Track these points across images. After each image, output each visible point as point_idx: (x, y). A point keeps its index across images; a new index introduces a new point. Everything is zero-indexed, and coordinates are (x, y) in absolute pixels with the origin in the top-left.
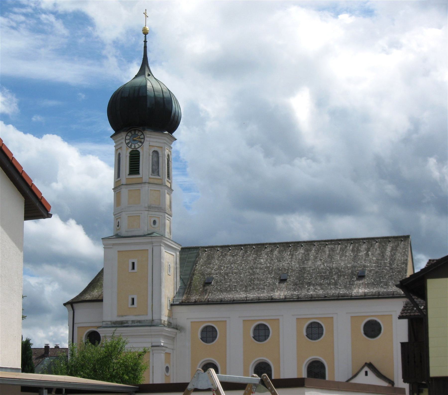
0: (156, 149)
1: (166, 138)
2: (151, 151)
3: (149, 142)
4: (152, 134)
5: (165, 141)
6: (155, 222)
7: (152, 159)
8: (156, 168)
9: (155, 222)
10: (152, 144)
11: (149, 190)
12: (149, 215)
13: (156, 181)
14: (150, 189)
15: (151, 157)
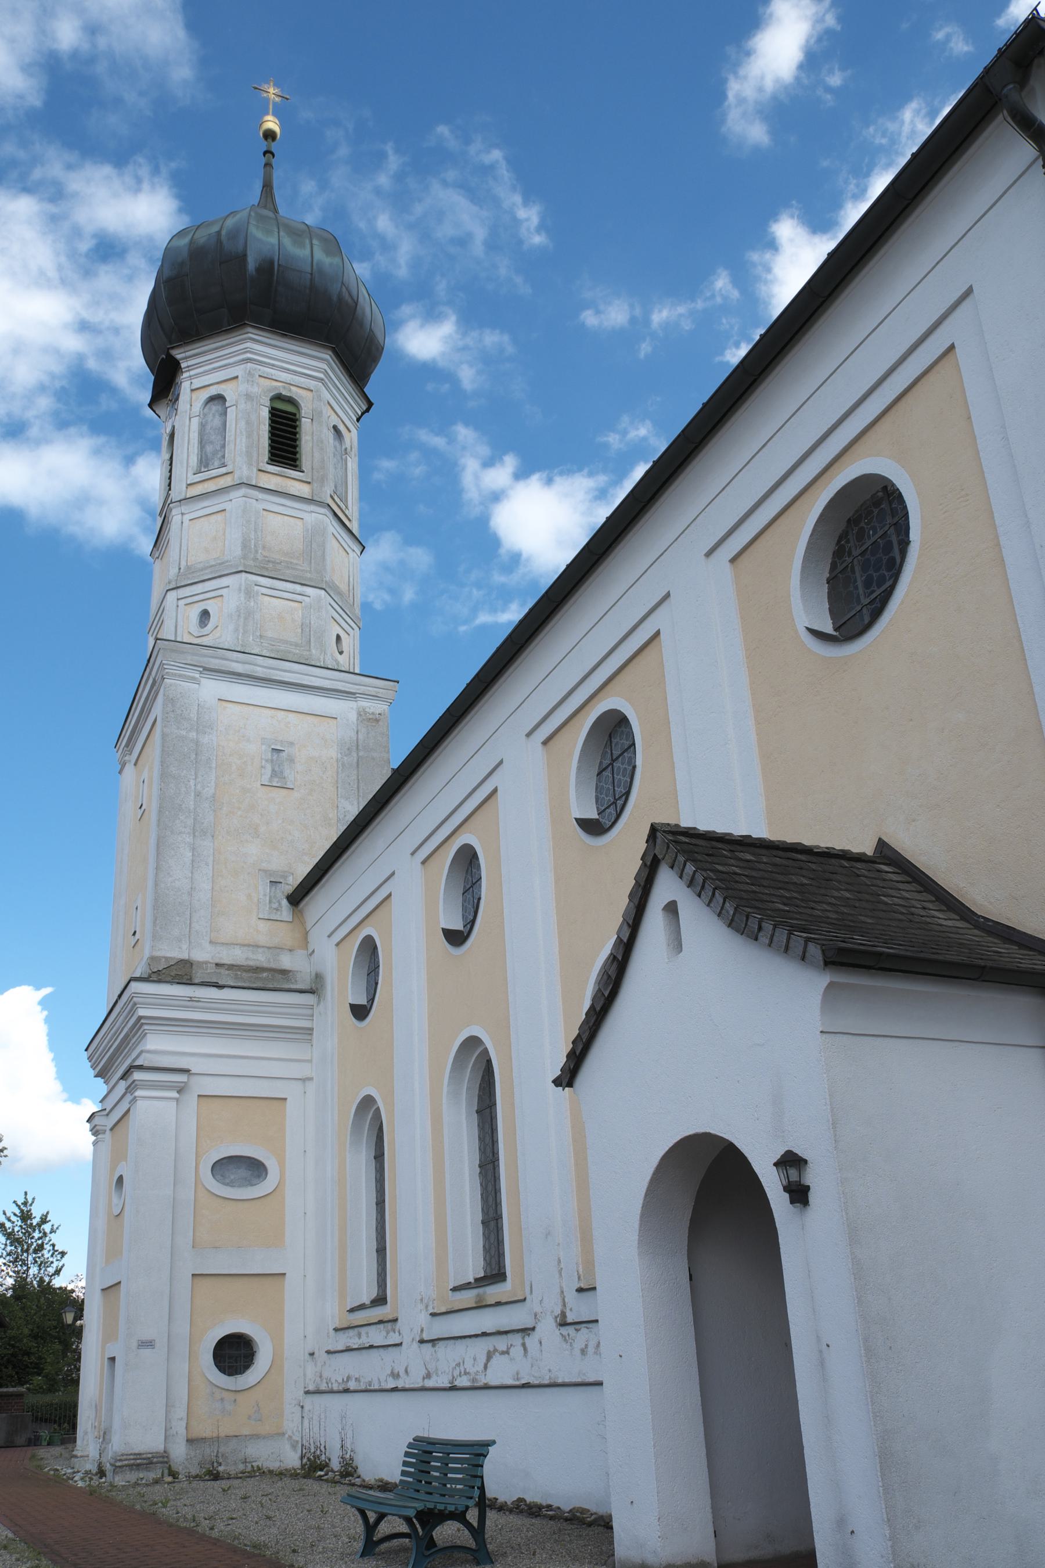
0: (213, 391)
1: (248, 344)
2: (198, 406)
3: (190, 382)
4: (188, 354)
5: (249, 355)
6: (205, 615)
7: (202, 426)
8: (218, 448)
9: (205, 615)
10: (197, 383)
11: (186, 523)
12: (182, 603)
13: (211, 486)
14: (187, 517)
15: (195, 421)
